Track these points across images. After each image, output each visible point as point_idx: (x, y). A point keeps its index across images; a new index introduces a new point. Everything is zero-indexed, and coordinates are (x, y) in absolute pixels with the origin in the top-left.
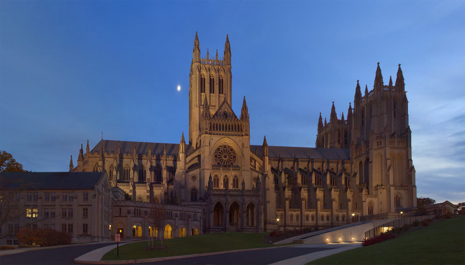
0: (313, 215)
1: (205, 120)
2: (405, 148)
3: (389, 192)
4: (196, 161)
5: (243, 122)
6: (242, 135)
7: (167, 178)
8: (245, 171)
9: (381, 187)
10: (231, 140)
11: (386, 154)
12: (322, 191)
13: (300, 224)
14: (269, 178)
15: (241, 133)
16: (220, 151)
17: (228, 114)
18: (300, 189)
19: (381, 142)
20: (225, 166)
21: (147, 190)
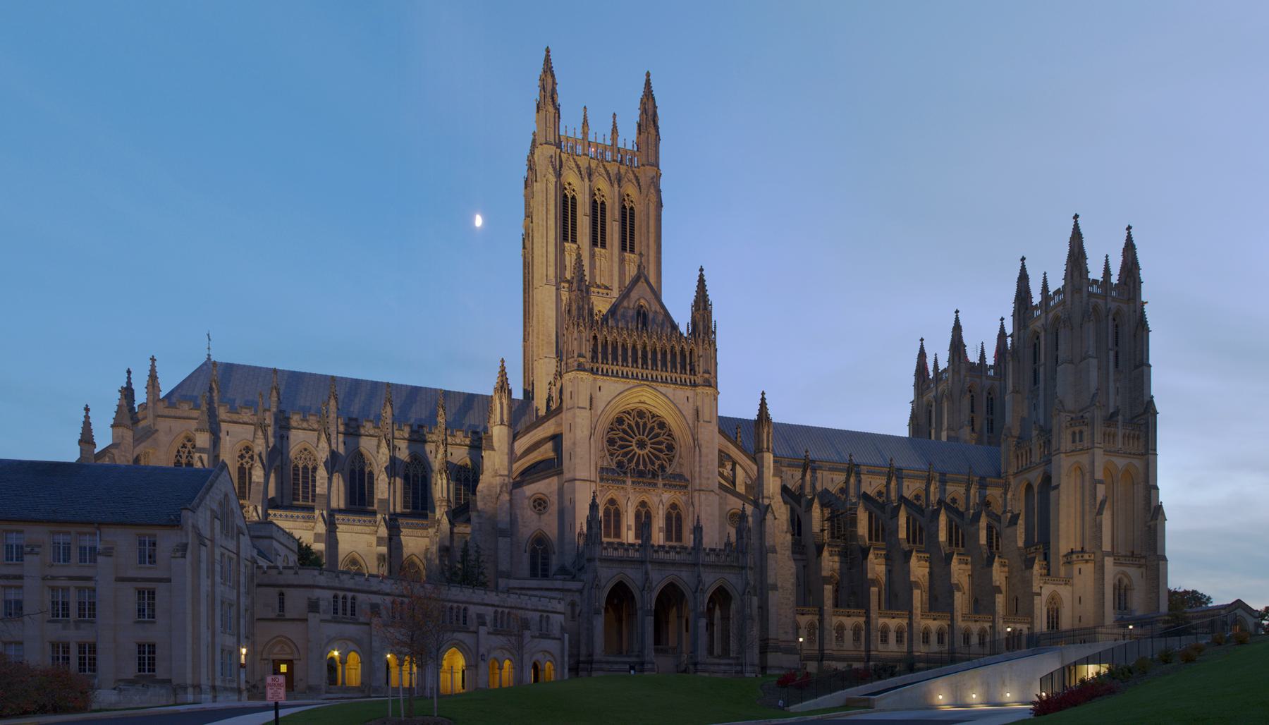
0: (899, 628)
1: (576, 327)
2: (1142, 455)
3: (1100, 569)
4: (547, 451)
5: (697, 344)
6: (693, 382)
7: (449, 501)
8: (701, 492)
9: (1080, 555)
10: (659, 395)
11: (1093, 466)
12: (926, 561)
13: (864, 653)
14: (774, 516)
15: (692, 378)
16: (625, 427)
17: (651, 316)
18: (865, 552)
19: (1081, 432)
20: (641, 474)
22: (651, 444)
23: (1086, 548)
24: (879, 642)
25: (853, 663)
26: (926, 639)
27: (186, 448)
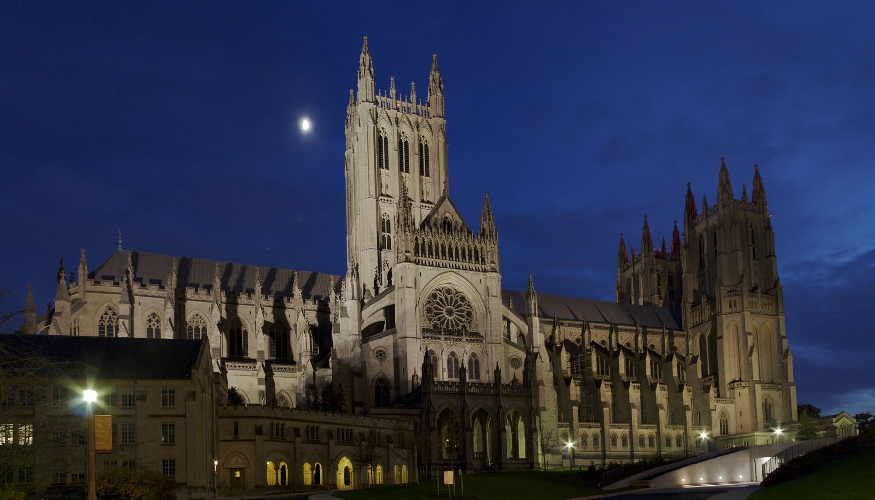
0: (623, 435)
1: (403, 232)
2: (774, 315)
3: (753, 393)
4: (380, 317)
5: (485, 243)
6: (484, 269)
7: (311, 351)
8: (493, 345)
9: (739, 383)
10: (461, 278)
11: (744, 324)
12: (638, 389)
13: (601, 453)
14: (542, 360)
15: (483, 266)
16: (438, 300)
17: (453, 224)
18: (598, 384)
19: (735, 301)
20: (449, 332)
21: (258, 379)
22: (456, 312)
23: (743, 378)
24: (611, 445)
25: (594, 460)
26: (642, 443)
27: (107, 314)
